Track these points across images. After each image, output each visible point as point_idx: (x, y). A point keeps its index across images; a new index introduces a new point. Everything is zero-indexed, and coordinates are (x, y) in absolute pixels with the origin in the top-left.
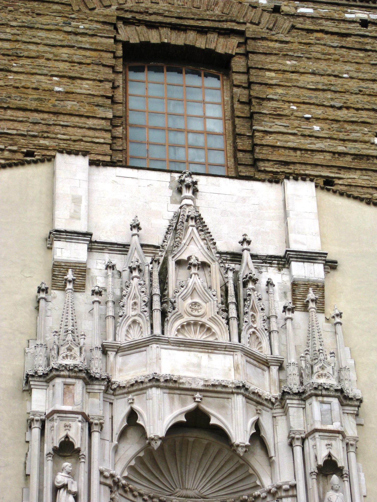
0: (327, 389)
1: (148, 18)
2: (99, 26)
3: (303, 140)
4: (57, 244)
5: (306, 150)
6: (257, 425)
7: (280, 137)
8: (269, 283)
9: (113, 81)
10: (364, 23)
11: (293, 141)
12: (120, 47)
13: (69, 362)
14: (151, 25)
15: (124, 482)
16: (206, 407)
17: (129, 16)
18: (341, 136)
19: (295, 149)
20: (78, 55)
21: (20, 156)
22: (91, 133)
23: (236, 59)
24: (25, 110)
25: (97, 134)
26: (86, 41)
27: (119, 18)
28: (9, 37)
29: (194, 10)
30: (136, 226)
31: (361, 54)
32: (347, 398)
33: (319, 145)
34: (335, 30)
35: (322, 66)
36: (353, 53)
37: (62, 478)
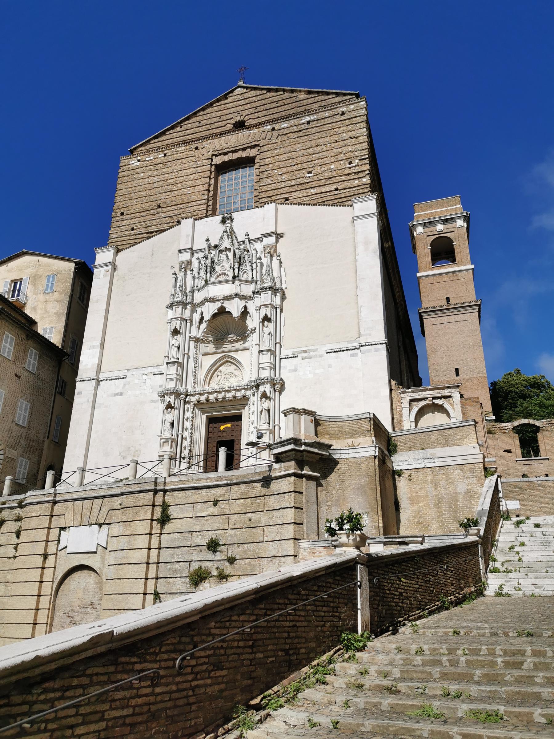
0: (266, 289)
1: (223, 151)
2: (205, 161)
3: (278, 184)
4: (180, 255)
5: (279, 189)
6: (245, 307)
7: (269, 186)
8: (255, 250)
9: (209, 183)
10: (309, 122)
11: (274, 186)
12: (213, 167)
13: (176, 300)
14: (225, 154)
15: (202, 338)
16: (224, 305)
17: (216, 153)
18: (293, 178)
19: (274, 190)
20: (196, 176)
21: (175, 224)
22: (199, 207)
23: (258, 156)
24: (178, 205)
25: (202, 206)
26: (200, 169)
27: (213, 155)
28: (174, 177)
29: (241, 141)
30: (208, 240)
31: (306, 137)
32: (276, 290)
33: (284, 184)
34: (295, 130)
35: (289, 149)
36: (302, 138)
37: (173, 342)
